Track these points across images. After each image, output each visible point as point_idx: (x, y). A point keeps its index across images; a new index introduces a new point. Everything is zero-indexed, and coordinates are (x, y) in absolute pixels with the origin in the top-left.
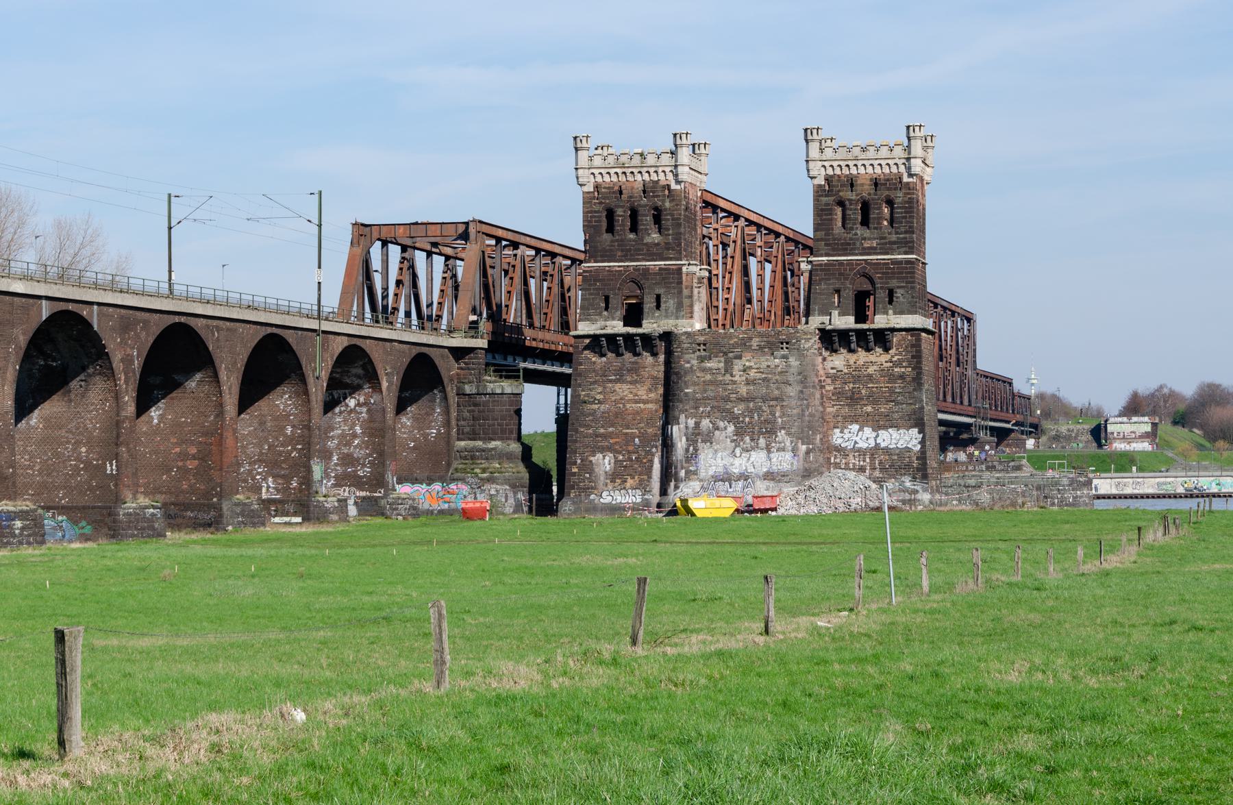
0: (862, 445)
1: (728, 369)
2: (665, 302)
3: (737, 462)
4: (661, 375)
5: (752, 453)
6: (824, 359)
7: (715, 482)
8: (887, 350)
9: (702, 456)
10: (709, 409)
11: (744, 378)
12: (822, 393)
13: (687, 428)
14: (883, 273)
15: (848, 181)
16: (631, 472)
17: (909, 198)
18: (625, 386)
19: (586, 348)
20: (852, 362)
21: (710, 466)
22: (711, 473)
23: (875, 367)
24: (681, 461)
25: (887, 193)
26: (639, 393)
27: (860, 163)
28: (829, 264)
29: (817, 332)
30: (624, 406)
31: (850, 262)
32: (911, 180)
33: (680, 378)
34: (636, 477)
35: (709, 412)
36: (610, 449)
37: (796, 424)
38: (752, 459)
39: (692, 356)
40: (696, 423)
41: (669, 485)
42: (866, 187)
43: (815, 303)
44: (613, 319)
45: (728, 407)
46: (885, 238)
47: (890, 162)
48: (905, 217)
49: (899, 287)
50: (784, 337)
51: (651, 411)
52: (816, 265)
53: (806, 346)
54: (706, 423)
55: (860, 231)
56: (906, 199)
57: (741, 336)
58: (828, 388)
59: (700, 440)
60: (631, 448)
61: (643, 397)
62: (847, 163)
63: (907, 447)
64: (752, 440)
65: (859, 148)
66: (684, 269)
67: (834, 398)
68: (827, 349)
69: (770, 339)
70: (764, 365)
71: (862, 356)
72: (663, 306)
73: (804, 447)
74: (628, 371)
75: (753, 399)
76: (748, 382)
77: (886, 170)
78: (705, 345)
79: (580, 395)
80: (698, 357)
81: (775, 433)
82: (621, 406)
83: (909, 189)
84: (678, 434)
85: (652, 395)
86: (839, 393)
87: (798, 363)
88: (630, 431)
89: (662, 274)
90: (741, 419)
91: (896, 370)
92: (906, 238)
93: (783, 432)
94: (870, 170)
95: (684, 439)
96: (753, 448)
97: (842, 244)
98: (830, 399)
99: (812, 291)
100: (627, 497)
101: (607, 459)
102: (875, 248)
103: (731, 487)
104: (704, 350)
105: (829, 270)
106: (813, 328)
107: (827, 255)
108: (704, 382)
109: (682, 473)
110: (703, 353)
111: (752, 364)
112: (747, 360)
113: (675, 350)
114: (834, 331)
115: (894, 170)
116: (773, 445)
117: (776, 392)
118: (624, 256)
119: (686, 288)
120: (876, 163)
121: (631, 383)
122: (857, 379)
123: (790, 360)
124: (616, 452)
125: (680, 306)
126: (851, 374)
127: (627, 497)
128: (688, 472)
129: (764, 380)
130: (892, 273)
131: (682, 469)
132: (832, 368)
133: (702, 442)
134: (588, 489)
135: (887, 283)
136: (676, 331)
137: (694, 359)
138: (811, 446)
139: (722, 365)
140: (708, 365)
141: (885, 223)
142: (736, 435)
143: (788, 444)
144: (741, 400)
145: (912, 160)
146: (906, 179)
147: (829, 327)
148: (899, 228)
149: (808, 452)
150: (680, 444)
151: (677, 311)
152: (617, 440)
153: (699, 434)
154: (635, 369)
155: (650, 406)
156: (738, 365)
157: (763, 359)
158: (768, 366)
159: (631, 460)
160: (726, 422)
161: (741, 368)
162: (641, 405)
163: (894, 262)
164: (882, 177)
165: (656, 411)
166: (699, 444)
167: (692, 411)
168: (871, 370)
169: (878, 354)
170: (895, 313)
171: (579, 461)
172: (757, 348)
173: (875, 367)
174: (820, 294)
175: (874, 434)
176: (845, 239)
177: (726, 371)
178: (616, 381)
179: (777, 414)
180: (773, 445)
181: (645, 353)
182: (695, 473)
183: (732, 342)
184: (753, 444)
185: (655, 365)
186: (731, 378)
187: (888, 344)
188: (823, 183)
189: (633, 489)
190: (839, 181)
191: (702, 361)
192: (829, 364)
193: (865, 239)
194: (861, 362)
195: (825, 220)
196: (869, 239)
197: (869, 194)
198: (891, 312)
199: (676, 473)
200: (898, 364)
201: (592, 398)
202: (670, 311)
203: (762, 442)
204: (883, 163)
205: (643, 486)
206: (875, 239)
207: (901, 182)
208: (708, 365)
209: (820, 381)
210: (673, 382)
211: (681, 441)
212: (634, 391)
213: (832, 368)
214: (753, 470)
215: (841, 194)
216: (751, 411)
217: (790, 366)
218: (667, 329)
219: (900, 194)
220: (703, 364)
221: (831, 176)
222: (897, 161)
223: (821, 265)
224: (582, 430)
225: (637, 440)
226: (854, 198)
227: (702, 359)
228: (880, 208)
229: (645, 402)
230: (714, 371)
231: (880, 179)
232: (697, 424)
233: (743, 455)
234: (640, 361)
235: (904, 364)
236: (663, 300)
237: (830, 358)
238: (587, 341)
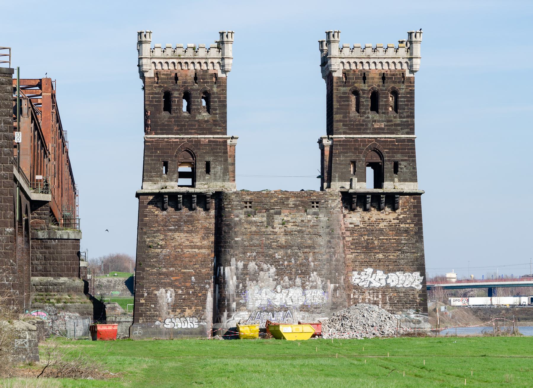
1: (270, 223)
2: (214, 168)
3: (278, 296)
4: (212, 227)
5: (291, 290)
6: (344, 216)
7: (261, 312)
8: (394, 209)
9: (249, 292)
10: (254, 254)
11: (283, 230)
12: (344, 243)
13: (237, 269)
14: (390, 149)
15: (361, 75)
16: (189, 303)
17: (410, 90)
18: (182, 235)
19: (150, 203)
20: (366, 219)
21: (257, 300)
22: (257, 305)
23: (385, 223)
24: (233, 295)
25: (392, 85)
26: (195, 240)
27: (371, 61)
28: (347, 140)
29: (340, 194)
31: (363, 140)
32: (412, 75)
33: (231, 229)
34: (193, 308)
35: (255, 257)
36: (171, 285)
37: (326, 267)
38: (290, 295)
39: (241, 211)
40: (244, 265)
41: (223, 314)
42: (376, 80)
43: (335, 172)
44: (171, 180)
45: (270, 252)
46: (391, 121)
47: (395, 60)
48: (407, 105)
49: (402, 160)
50: (315, 198)
51: (204, 254)
52: (336, 141)
53: (333, 205)
54: (252, 265)
55: (371, 115)
56: (408, 90)
57: (280, 196)
58: (347, 239)
59: (248, 279)
60: (188, 284)
61: (198, 244)
64: (290, 279)
65: (371, 49)
66: (229, 141)
67: (352, 247)
68: (346, 208)
69: (304, 199)
70: (299, 219)
71: (374, 214)
72: (212, 171)
73: (332, 285)
74: (185, 222)
75: (291, 247)
76: (286, 233)
77: (392, 67)
78: (250, 203)
79: (145, 241)
80: (245, 212)
81: (309, 274)
82: (180, 250)
83: (411, 83)
84: (230, 274)
85: (205, 242)
86: (357, 243)
87: (327, 218)
88: (188, 271)
89: (211, 145)
90: (281, 263)
91: (402, 226)
92: (408, 121)
93: (315, 273)
94: (379, 66)
95: (235, 278)
96: (291, 286)
97: (357, 125)
98: (349, 247)
99: (333, 162)
100: (186, 324)
101: (169, 292)
102: (383, 129)
103: (273, 316)
104: (250, 207)
105: (346, 145)
106: (337, 191)
107: (345, 133)
108: (250, 232)
109: (234, 305)
110: (249, 210)
111: (289, 219)
112: (285, 216)
113: (225, 206)
114: (355, 193)
115: (399, 67)
116: (307, 283)
117: (309, 242)
118: (181, 130)
119: (230, 157)
120: (384, 61)
121: (187, 232)
122: (371, 232)
123: (320, 216)
124: (176, 287)
125: (226, 171)
127: (186, 324)
128: (238, 304)
129: (299, 231)
130: (397, 149)
131: (234, 301)
132: (351, 224)
133: (250, 280)
134: (154, 316)
135: (393, 157)
136: (226, 191)
137: (242, 214)
138: (337, 285)
139: (265, 219)
140: (254, 219)
141: (390, 109)
142: (277, 275)
143: (319, 283)
144: (281, 247)
145: (414, 60)
146: (408, 74)
147: (351, 191)
148: (402, 113)
149: (335, 290)
150: (232, 282)
151: (224, 176)
152: (177, 278)
153: (247, 274)
154: (190, 221)
155: (203, 251)
156: (278, 220)
157: (298, 215)
158: (302, 221)
159: (189, 294)
160: (269, 265)
161: (281, 222)
162: (196, 250)
163: (399, 140)
164: (389, 72)
165: (209, 255)
166: (247, 282)
167: (241, 255)
168: (382, 225)
169: (387, 213)
170: (400, 181)
171: (146, 294)
172: (293, 206)
173: (385, 223)
174: (340, 164)
176: (359, 121)
177: (268, 224)
178: (175, 231)
179: (310, 259)
180: (307, 283)
181: (198, 209)
182: (244, 305)
183: (272, 201)
184: (291, 282)
185: (207, 218)
186: (272, 230)
187: (396, 205)
188: (341, 76)
189: (191, 317)
190: (354, 74)
191: (249, 216)
192: (348, 220)
193: (375, 121)
194: (374, 219)
195: (343, 105)
196: (379, 121)
197: (379, 86)
198: (396, 180)
199: (229, 305)
200: (402, 221)
201: (155, 243)
202: (218, 175)
203: (298, 281)
204: (390, 61)
205: (199, 315)
206: (383, 121)
207: (403, 77)
208: (254, 219)
209: (342, 233)
210: (225, 232)
211: (232, 279)
212: (190, 239)
213: (351, 224)
214: (291, 303)
215: (356, 85)
216: (289, 256)
217: (320, 221)
218: (218, 189)
219: (403, 86)
220: (249, 218)
221: (348, 71)
222: (401, 60)
223: (340, 141)
224: (148, 269)
225: (193, 278)
226: (366, 88)
227: (248, 215)
228: (387, 97)
229: (200, 248)
230: (259, 224)
231: (387, 74)
232: (245, 266)
233: (283, 291)
234: (194, 214)
236: (212, 166)
237: (349, 215)
238: (151, 198)
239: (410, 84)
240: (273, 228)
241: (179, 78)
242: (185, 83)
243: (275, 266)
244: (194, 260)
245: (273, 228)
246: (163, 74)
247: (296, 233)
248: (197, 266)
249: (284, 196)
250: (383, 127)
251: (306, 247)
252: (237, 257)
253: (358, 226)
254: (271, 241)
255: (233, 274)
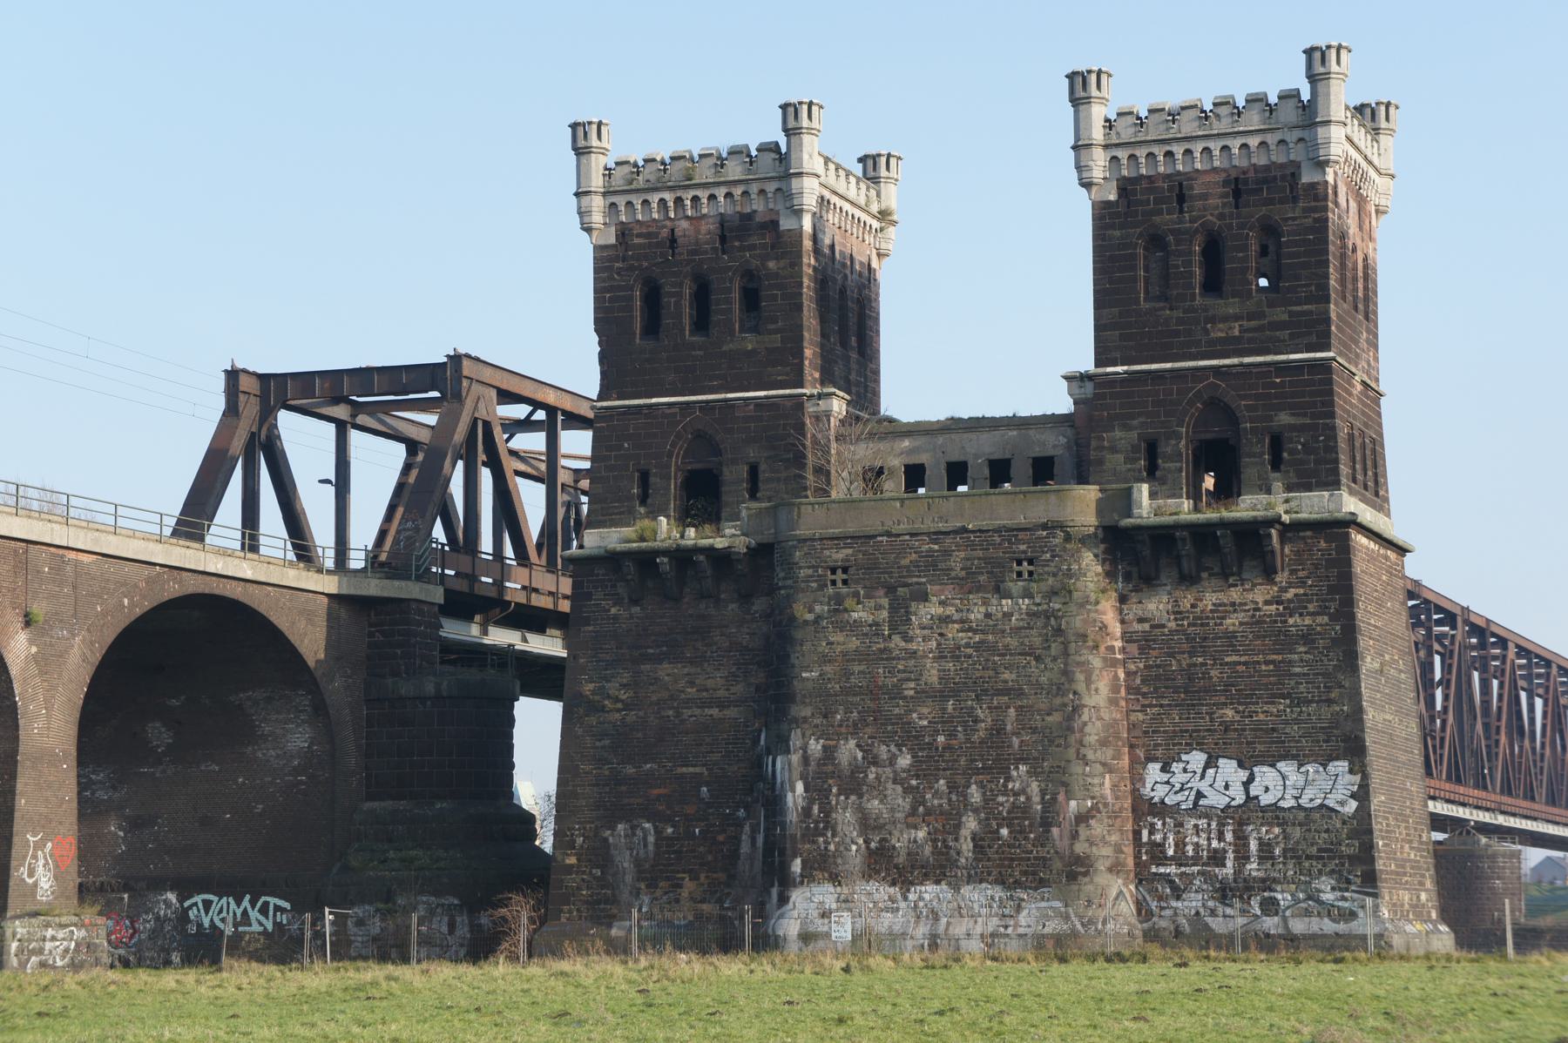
0: (1215, 800)
8: (1269, 573)
13: (806, 760)
15: (1170, 189)
20: (1186, 604)
30: (678, 715)
34: (702, 876)
50: (1023, 547)
62: (1168, 148)
63: (1322, 806)
78: (845, 570)
82: (671, 713)
83: (1316, 198)
85: (739, 689)
86: (1158, 677)
88: (691, 770)
91: (1291, 621)
93: (1023, 768)
102: (1237, 340)
104: (845, 582)
108: (844, 654)
109: (797, 866)
116: (1001, 799)
122: (1197, 645)
126: (1184, 632)
129: (978, 647)
132: (1141, 620)
139: (885, 614)
155: (731, 712)
162: (715, 712)
168: (1232, 622)
175: (1243, 775)
197: (1221, 216)
198: (1278, 486)
206: (1237, 318)
211: (793, 791)
213: (1141, 620)
215: (1157, 219)
229: (722, 705)
231: (1246, 182)
232: (829, 753)
235: (1311, 607)
239: (1313, 204)
240: (907, 638)
241: (680, 241)
242: (695, 252)
243: (910, 750)
244: (708, 740)
245: (907, 638)
246: (638, 236)
247: (969, 651)
248: (716, 757)
249: (936, 547)
250: (1236, 333)
251: (1000, 693)
252: (806, 726)
253: (1163, 626)
254: (901, 676)
255: (796, 774)
